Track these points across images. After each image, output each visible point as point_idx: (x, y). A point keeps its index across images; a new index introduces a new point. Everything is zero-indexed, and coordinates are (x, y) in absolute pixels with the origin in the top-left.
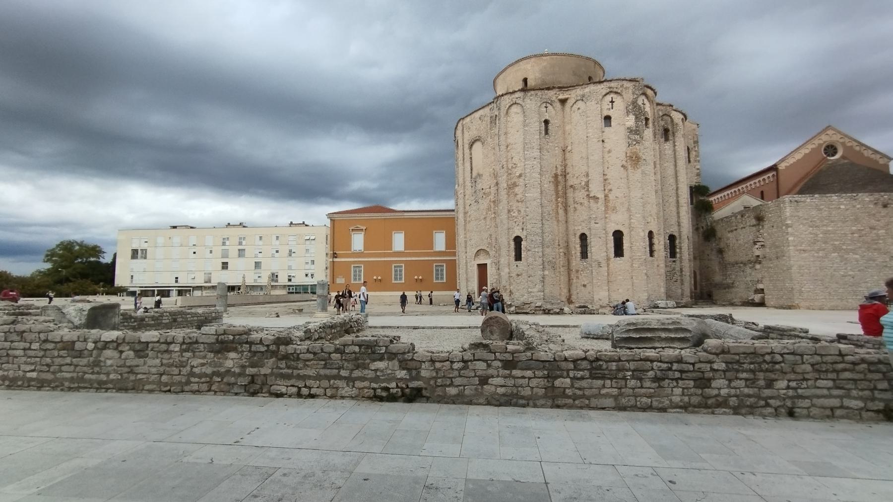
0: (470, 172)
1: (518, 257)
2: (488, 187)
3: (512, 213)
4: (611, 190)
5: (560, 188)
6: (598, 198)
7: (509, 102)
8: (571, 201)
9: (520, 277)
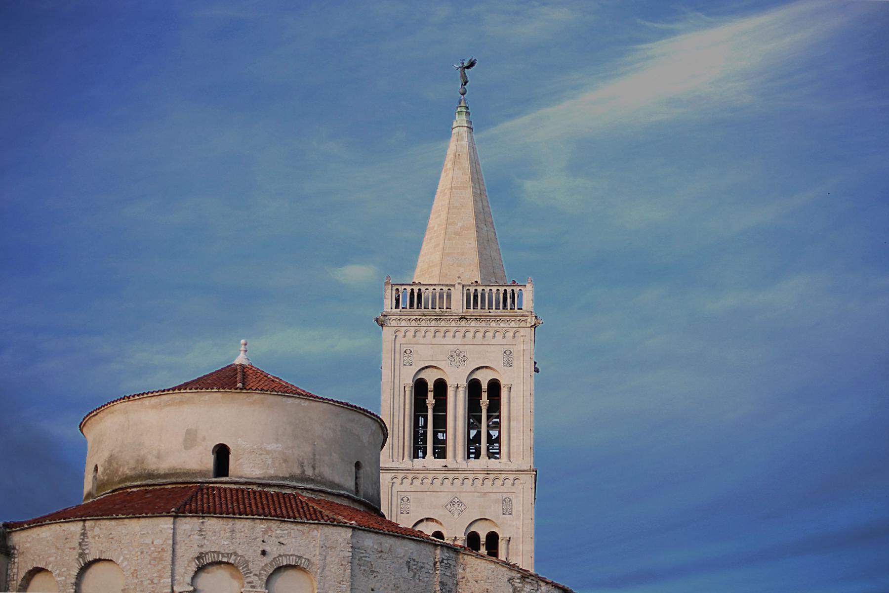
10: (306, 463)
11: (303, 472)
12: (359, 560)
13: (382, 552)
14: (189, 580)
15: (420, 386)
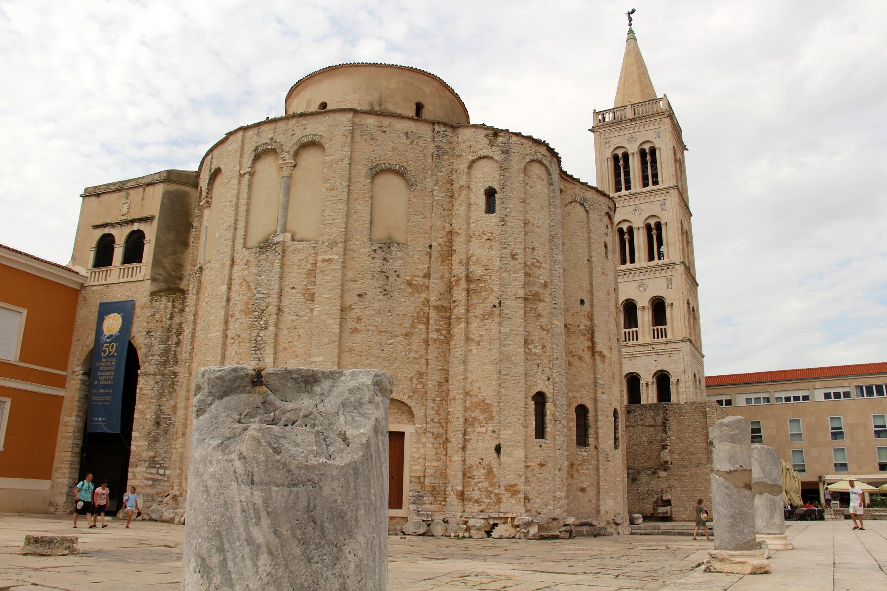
0: (367, 225)
2: (422, 274)
3: (531, 347)
6: (605, 356)
7: (531, 154)
9: (544, 468)
10: (374, 103)
11: (372, 108)
12: (361, 132)
13: (382, 126)
14: (249, 165)
15: (616, 158)
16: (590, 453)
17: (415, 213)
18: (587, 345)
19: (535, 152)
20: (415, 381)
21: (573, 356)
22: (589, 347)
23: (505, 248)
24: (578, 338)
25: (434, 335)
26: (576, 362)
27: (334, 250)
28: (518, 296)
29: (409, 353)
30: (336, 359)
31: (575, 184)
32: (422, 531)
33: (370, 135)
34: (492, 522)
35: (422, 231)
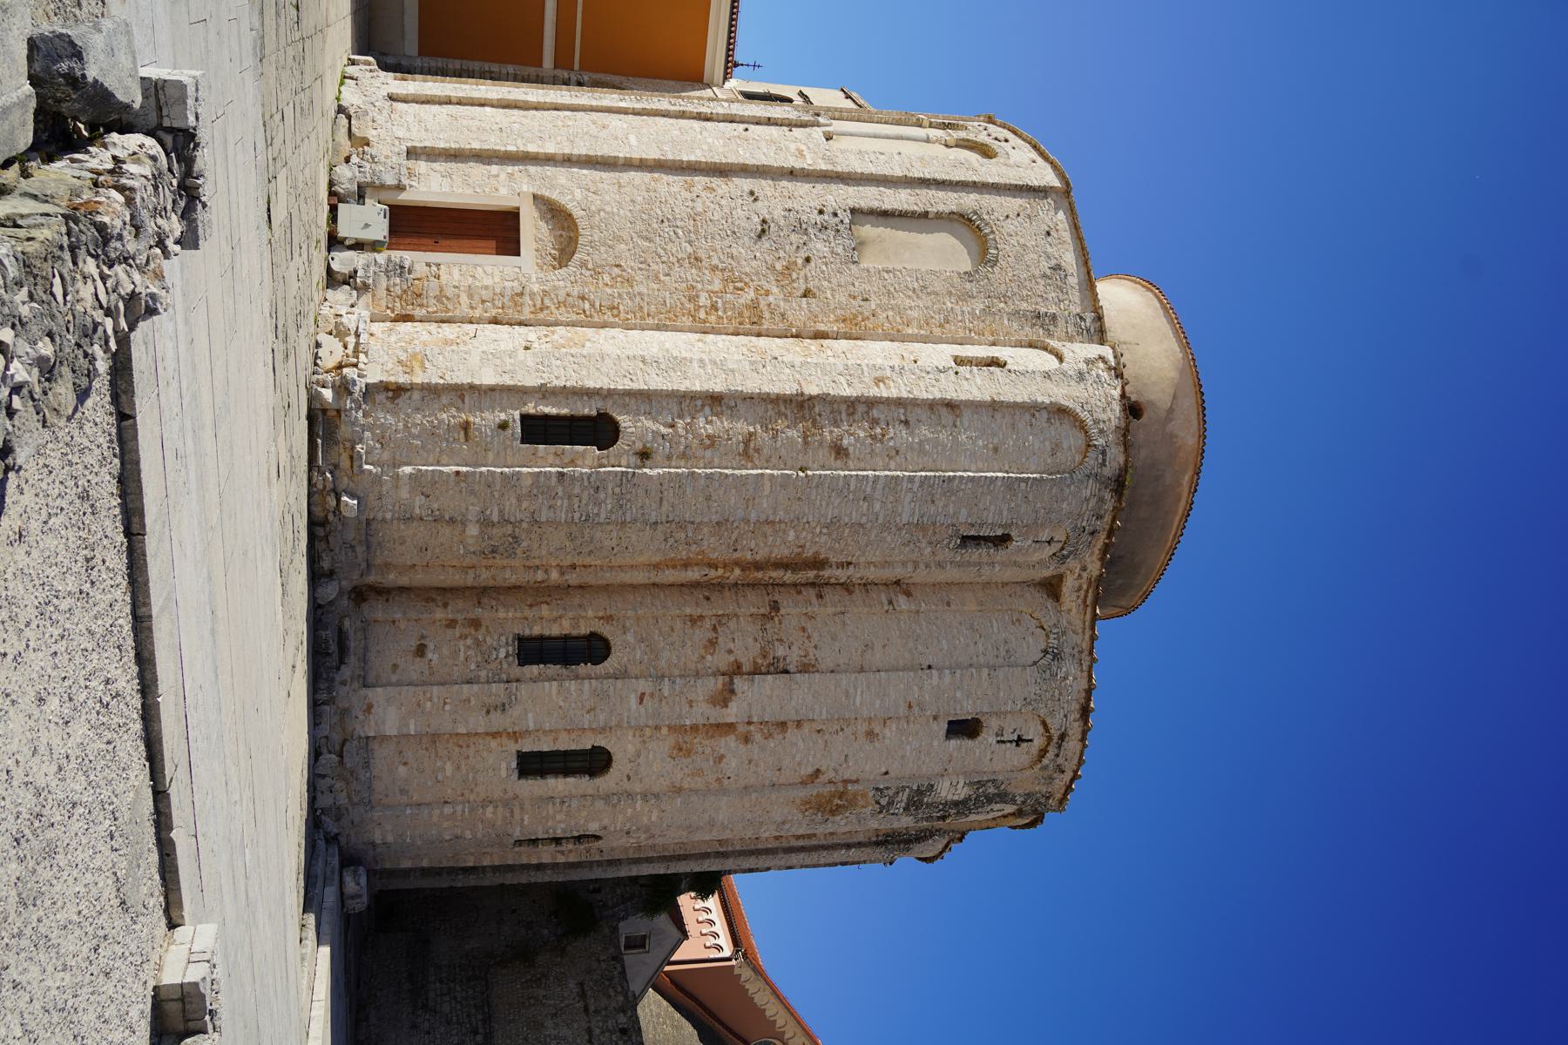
1: (538, 430)
3: (707, 409)
4: (747, 739)
5: (776, 574)
6: (727, 706)
7: (1096, 422)
8: (723, 604)
16: (505, 666)
17: (919, 276)
18: (743, 660)
19: (1101, 431)
20: (616, 271)
21: (715, 629)
22: (739, 666)
23: (892, 368)
24: (756, 640)
25: (703, 300)
26: (702, 634)
27: (820, 161)
28: (803, 384)
29: (663, 262)
30: (636, 155)
31: (1083, 632)
32: (335, 266)
33: (1035, 213)
34: (351, 340)
35: (892, 290)
